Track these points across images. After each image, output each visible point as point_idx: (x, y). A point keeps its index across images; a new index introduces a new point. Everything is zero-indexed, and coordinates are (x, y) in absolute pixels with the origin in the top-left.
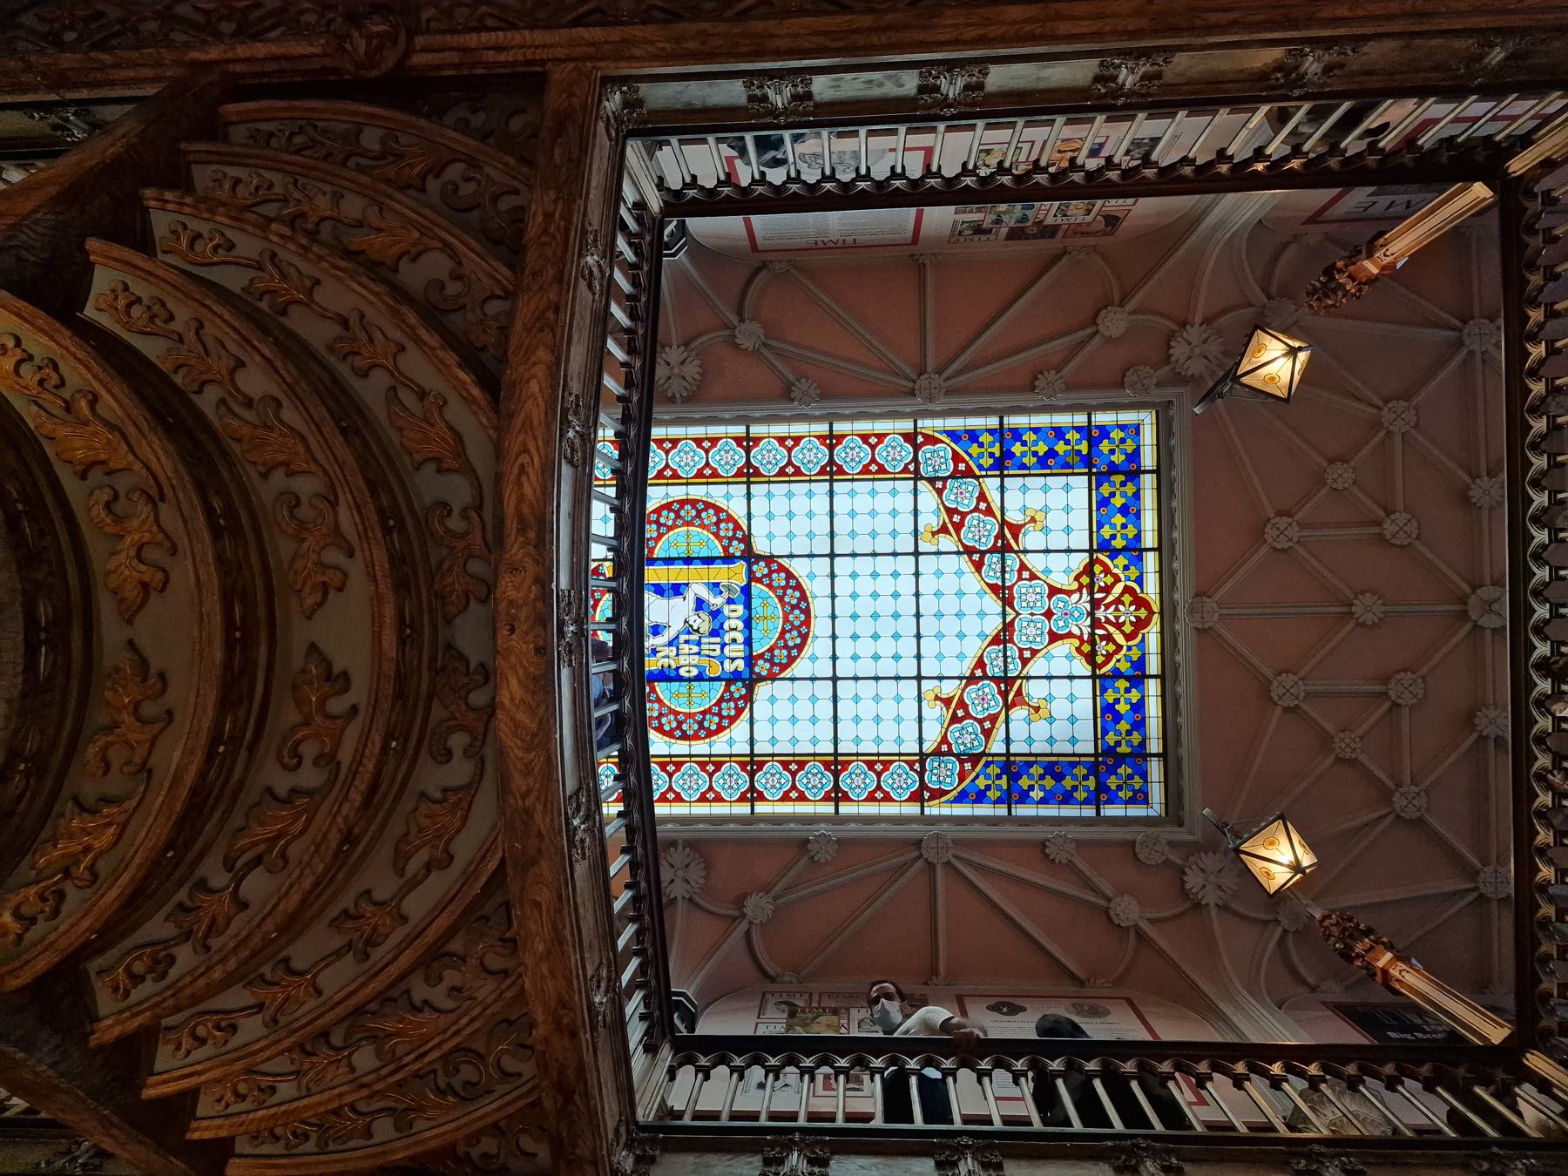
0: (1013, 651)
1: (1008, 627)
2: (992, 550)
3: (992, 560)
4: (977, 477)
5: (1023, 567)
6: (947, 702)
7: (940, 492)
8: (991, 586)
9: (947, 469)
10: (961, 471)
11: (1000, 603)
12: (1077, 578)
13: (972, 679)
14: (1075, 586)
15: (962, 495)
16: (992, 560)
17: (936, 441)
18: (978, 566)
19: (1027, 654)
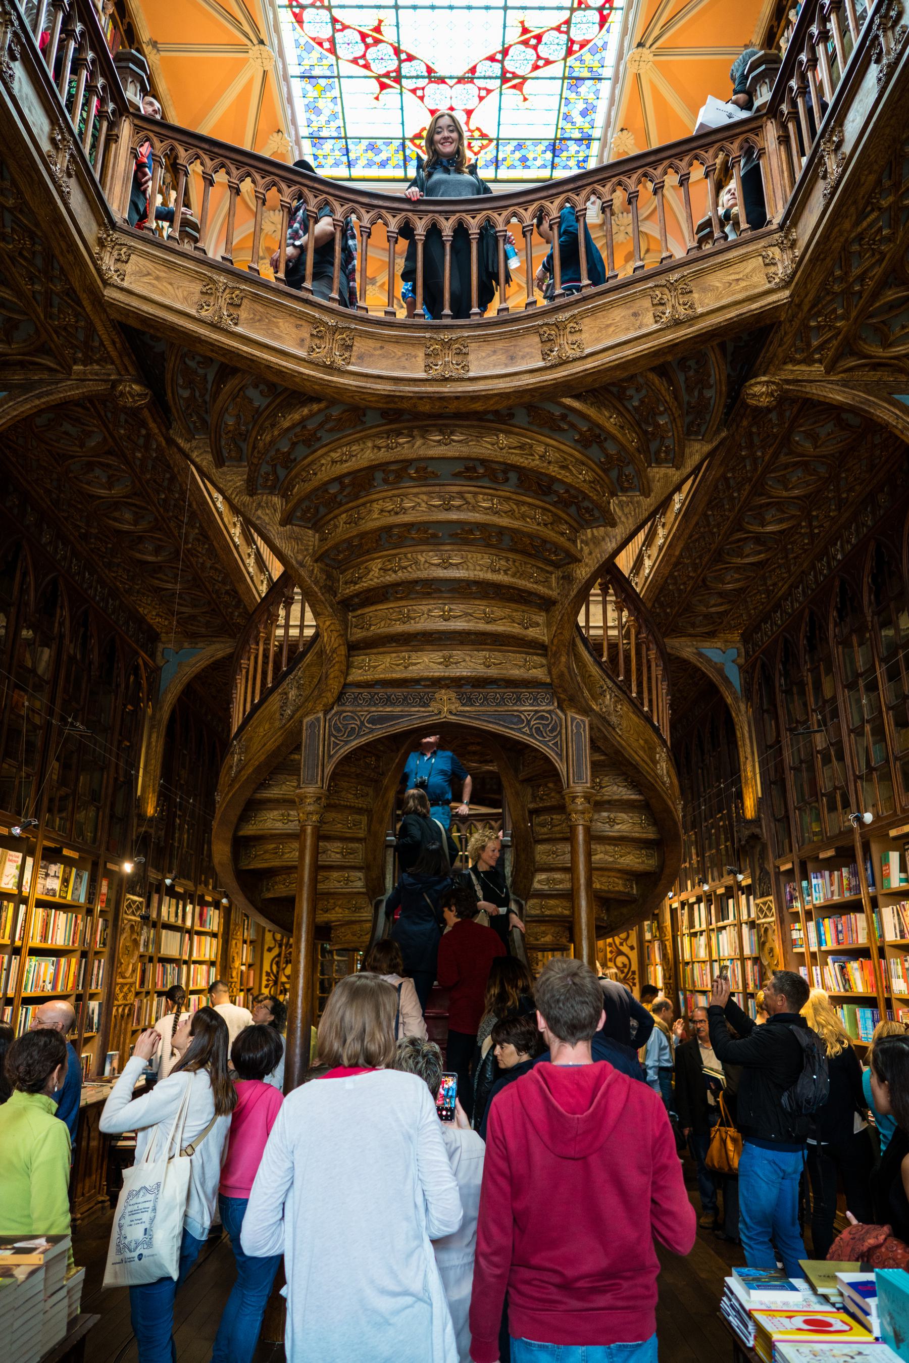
0: (422, 83)
1: (442, 80)
2: (503, 68)
3: (496, 69)
4: (565, 59)
5: (489, 91)
6: (377, 29)
7: (558, 29)
8: (473, 70)
9: (577, 34)
10: (572, 46)
11: (460, 74)
12: (478, 129)
13: (397, 51)
14: (472, 127)
15: (553, 47)
16: (496, 69)
17: (601, 26)
18: (492, 59)
19: (419, 93)
